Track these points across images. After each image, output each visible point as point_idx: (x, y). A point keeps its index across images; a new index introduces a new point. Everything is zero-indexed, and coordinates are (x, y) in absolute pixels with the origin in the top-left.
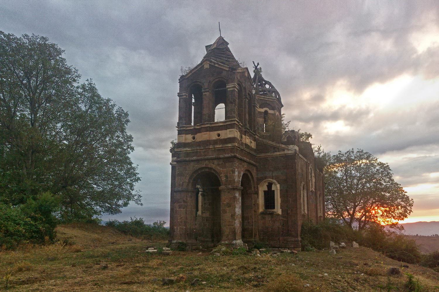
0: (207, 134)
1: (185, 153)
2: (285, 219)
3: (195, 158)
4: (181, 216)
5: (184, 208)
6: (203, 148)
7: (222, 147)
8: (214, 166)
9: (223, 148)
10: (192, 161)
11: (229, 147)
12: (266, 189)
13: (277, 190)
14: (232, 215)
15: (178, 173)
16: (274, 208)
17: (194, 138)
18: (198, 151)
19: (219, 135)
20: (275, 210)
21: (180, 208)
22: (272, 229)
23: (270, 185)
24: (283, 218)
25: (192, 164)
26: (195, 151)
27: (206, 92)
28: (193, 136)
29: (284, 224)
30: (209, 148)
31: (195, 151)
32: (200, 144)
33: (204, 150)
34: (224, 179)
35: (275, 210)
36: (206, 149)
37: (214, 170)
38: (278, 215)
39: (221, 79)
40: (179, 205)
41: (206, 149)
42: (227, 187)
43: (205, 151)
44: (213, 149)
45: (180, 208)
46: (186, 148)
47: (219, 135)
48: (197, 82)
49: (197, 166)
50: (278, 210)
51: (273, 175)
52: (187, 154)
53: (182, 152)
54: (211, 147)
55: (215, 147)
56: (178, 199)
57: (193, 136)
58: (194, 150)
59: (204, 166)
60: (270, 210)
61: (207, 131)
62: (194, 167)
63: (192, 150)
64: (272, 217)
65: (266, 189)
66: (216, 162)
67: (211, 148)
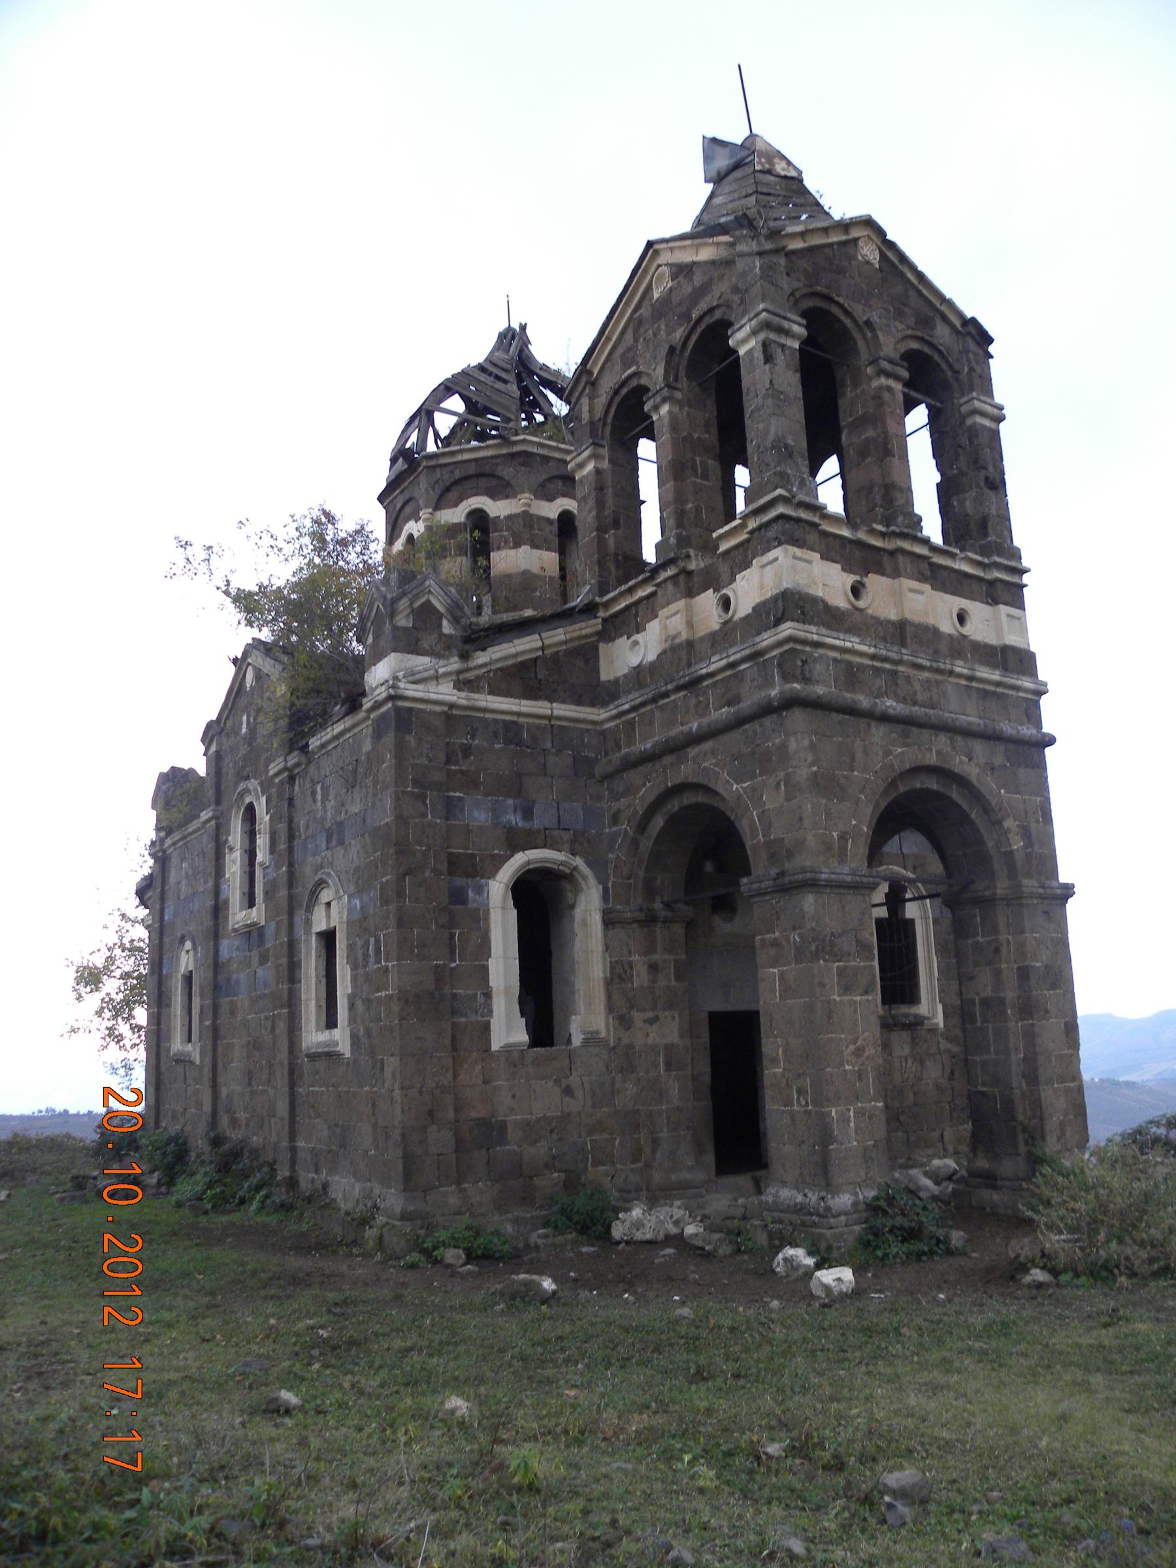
0: (921, 593)
1: (835, 660)
2: (956, 1049)
3: (890, 704)
4: (855, 1041)
5: (866, 992)
6: (928, 664)
7: (998, 684)
8: (972, 772)
9: (1000, 690)
10: (884, 718)
11: (1021, 694)
12: (883, 912)
13: (926, 918)
14: (1066, 1024)
15: (815, 773)
16: (912, 997)
17: (856, 590)
18: (901, 668)
19: (962, 618)
20: (923, 1009)
21: (846, 989)
22: (915, 1094)
23: (895, 900)
24: (949, 1046)
25: (878, 732)
26: (887, 666)
27: (897, 378)
28: (857, 578)
29: (952, 1073)
30: (951, 673)
31: (887, 666)
32: (901, 632)
33: (926, 675)
34: (1017, 844)
35: (923, 1009)
36: (938, 671)
37: (977, 797)
38: (933, 1030)
39: (926, 349)
40: (841, 972)
41: (938, 671)
42: (1043, 887)
43: (928, 681)
44: (963, 682)
45: (846, 989)
46: (847, 637)
47: (962, 618)
48: (830, 299)
49: (904, 755)
50: (930, 1007)
51: (905, 850)
52: (851, 674)
53: (821, 651)
54: (960, 668)
55: (978, 674)
56: (832, 935)
57: (857, 578)
58: (885, 659)
59: (932, 759)
60: (904, 1009)
61: (922, 578)
62: (887, 753)
63: (873, 657)
64: (914, 1043)
65: (883, 912)
66: (978, 747)
67: (960, 676)
